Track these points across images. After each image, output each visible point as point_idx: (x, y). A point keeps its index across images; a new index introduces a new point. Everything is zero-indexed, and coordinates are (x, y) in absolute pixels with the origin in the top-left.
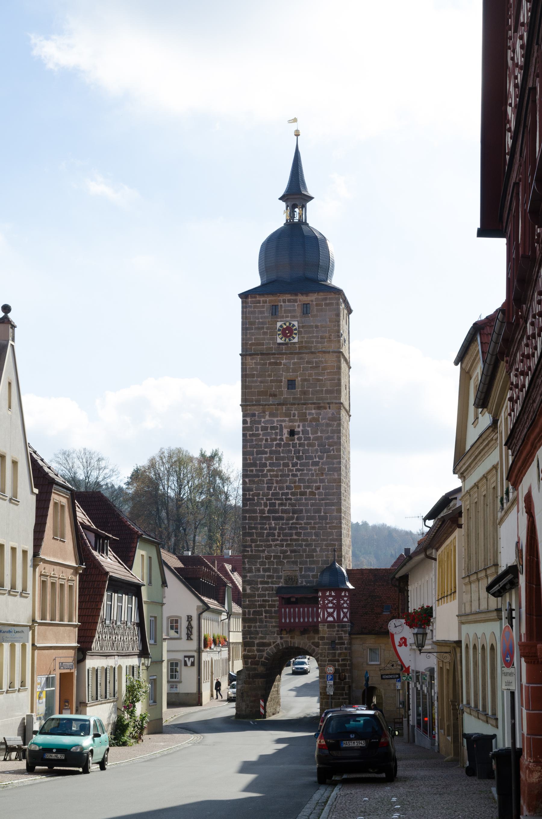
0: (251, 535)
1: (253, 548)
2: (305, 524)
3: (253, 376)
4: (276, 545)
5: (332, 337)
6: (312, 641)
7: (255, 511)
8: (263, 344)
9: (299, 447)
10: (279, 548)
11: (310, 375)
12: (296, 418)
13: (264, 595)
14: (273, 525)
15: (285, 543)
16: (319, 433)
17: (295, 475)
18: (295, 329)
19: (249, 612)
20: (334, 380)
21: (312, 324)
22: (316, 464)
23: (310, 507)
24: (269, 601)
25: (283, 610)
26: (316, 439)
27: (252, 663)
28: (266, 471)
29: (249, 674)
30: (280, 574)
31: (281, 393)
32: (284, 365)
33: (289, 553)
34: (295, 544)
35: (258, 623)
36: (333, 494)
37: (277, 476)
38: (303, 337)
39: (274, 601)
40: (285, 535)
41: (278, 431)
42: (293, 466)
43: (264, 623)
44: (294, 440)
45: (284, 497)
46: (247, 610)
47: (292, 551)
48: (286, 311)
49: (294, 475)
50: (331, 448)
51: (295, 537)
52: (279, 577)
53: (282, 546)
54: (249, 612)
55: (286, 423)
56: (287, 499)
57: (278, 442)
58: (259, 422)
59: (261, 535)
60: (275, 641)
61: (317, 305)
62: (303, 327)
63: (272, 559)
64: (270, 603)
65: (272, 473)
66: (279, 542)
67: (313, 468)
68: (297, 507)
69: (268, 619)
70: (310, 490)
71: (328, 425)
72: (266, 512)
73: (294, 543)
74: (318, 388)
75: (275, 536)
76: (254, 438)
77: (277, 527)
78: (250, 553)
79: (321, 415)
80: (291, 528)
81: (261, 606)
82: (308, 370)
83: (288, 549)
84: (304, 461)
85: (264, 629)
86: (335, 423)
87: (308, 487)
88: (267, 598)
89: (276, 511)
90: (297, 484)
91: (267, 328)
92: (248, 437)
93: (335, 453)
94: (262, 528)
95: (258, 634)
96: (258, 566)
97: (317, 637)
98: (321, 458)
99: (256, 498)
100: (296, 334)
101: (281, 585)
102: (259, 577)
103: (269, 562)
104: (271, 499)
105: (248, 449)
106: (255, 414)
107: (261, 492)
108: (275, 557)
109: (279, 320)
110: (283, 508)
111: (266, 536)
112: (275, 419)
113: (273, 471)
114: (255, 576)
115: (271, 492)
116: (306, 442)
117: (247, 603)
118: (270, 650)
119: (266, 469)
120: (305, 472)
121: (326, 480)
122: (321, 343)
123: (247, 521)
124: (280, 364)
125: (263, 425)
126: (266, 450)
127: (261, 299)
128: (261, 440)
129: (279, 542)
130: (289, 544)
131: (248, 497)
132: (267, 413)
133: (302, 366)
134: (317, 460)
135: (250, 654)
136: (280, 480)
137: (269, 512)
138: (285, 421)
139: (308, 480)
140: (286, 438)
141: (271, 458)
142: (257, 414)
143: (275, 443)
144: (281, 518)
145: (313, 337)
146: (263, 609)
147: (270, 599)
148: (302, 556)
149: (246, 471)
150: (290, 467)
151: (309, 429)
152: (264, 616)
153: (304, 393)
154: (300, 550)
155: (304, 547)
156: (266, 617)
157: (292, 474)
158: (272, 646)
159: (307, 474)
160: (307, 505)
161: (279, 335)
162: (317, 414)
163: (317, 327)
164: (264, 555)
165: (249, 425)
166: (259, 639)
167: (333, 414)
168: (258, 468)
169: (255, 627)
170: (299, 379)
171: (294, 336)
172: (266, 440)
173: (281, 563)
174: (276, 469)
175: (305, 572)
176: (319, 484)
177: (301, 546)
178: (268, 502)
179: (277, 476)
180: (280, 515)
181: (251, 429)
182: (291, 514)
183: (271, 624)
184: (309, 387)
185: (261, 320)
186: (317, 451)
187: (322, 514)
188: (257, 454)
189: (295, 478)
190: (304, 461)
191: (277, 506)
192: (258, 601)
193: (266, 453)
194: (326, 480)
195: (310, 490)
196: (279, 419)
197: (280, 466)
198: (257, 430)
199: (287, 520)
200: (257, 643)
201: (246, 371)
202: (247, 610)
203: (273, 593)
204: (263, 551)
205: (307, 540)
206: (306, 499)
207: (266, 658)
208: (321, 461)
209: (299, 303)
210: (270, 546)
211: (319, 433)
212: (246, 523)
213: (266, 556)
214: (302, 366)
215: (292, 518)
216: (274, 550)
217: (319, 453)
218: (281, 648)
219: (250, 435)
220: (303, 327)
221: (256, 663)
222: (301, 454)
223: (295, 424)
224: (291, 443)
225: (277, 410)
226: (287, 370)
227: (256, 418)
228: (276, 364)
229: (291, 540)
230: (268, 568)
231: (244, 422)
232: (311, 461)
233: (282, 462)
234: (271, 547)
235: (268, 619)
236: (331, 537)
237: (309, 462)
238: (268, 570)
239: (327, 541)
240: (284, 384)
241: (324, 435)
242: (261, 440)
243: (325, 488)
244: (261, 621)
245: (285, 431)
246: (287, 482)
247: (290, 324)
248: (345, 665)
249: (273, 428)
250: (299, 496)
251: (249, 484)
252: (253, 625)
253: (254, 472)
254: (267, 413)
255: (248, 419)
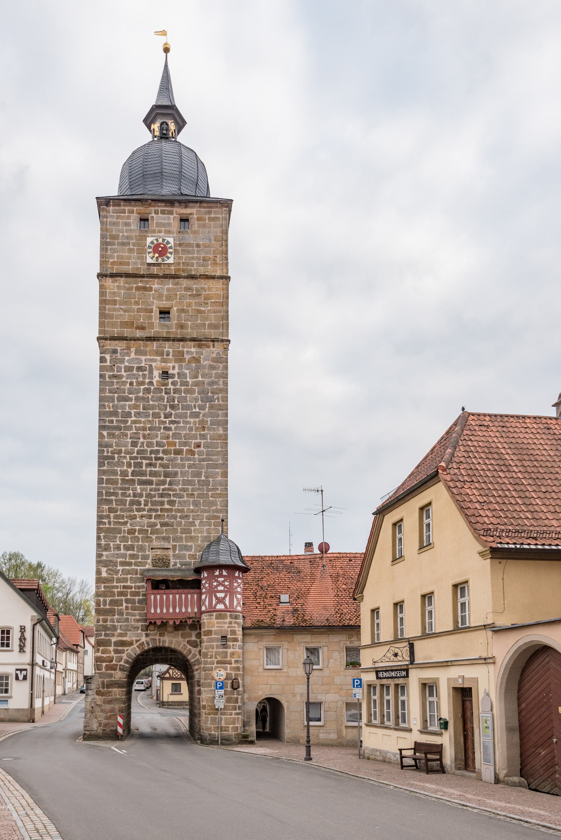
0: (110, 502)
1: (112, 520)
2: (181, 490)
3: (115, 302)
4: (142, 516)
5: (218, 259)
6: (187, 640)
7: (115, 473)
8: (128, 264)
9: (174, 393)
10: (145, 520)
11: (189, 305)
12: (171, 357)
13: (126, 580)
14: (139, 491)
15: (154, 514)
16: (200, 377)
17: (169, 429)
18: (171, 248)
19: (105, 601)
20: (219, 312)
21: (192, 242)
22: (196, 415)
23: (187, 469)
24: (131, 588)
25: (152, 597)
26: (197, 384)
27: (107, 668)
28: (130, 422)
29: (103, 683)
30: (147, 553)
31: (152, 325)
32: (156, 291)
33: (159, 527)
34: (168, 515)
35: (117, 616)
36: (218, 453)
37: (144, 429)
38: (180, 258)
39: (139, 587)
40: (154, 503)
41: (146, 373)
42: (165, 417)
43: (125, 616)
44: (167, 385)
45: (153, 456)
46: (102, 599)
47: (162, 525)
48: (158, 225)
49: (167, 429)
50: (215, 397)
51: (167, 506)
52: (145, 557)
53: (150, 517)
54: (105, 601)
55: (158, 364)
56: (156, 459)
57: (146, 386)
58: (122, 361)
59: (123, 502)
60: (138, 639)
61: (199, 219)
62: (180, 245)
63: (136, 534)
64: (133, 590)
65: (137, 425)
66: (145, 513)
67: (192, 420)
68: (171, 469)
69: (130, 611)
70: (187, 448)
71: (212, 367)
72: (130, 474)
73: (166, 514)
74: (199, 322)
75: (141, 505)
76: (115, 381)
77: (144, 493)
78: (107, 526)
79: (202, 354)
80: (162, 496)
81: (121, 594)
82: (186, 299)
83: (158, 521)
84: (180, 411)
85: (125, 624)
86: (221, 366)
87: (185, 444)
88: (129, 584)
89: (143, 474)
90: (171, 440)
91: (134, 245)
92: (107, 379)
93: (221, 402)
94: (123, 495)
95: (116, 630)
96: (118, 542)
97: (194, 633)
98: (202, 408)
99: (116, 456)
100: (171, 253)
101: (147, 567)
102: (118, 556)
103: (131, 538)
104: (136, 458)
105: (107, 394)
106: (117, 350)
107: (123, 449)
108: (140, 531)
109: (150, 235)
110: (152, 469)
111: (129, 504)
112: (143, 358)
113: (140, 422)
114: (113, 555)
115: (136, 449)
116: (183, 388)
117: (103, 589)
118: (133, 651)
119: (129, 420)
120: (182, 425)
121: (208, 437)
122: (203, 266)
123: (104, 485)
124: (150, 289)
125: (127, 364)
126: (131, 396)
127: (127, 208)
128: (124, 383)
129: (145, 513)
130: (160, 515)
131: (105, 454)
132: (133, 350)
133: (178, 293)
134: (197, 410)
135: (105, 655)
136: (149, 435)
137: (133, 474)
138: (155, 361)
139: (186, 435)
140: (157, 381)
141: (136, 407)
142: (119, 351)
143: (142, 387)
144: (150, 483)
145: (193, 258)
146: (124, 598)
147: (133, 585)
148: (175, 531)
149: (104, 421)
150: (162, 419)
151: (187, 372)
152: (124, 607)
153: (182, 327)
154: (173, 523)
155: (178, 519)
156: (127, 608)
157: (164, 428)
158: (135, 646)
159: (184, 428)
160: (183, 466)
161: (149, 253)
162: (197, 352)
163: (198, 246)
164: (126, 529)
165: (108, 364)
166: (118, 636)
167: (218, 353)
168: (120, 418)
169: (112, 620)
170: (175, 309)
171: (169, 255)
172: (131, 384)
173: (148, 539)
174: (143, 420)
175: (179, 550)
176: (199, 441)
177: (175, 517)
178: (132, 461)
179: (144, 429)
180: (148, 478)
181: (111, 368)
182: (162, 478)
183: (133, 618)
184: (188, 320)
185: (125, 234)
186: (196, 400)
187: (203, 478)
188: (119, 401)
189: (169, 432)
190: (180, 411)
191: (144, 466)
192: (117, 587)
193: (131, 400)
194: (208, 437)
195: (187, 448)
196: (148, 357)
197: (148, 416)
198: (119, 370)
199: (156, 485)
200: (115, 642)
201: (106, 296)
202: (102, 599)
203: (137, 578)
204: (126, 523)
205: (182, 511)
206: (182, 459)
207: (127, 662)
208: (202, 412)
209: (175, 215)
210: (135, 517)
211: (200, 377)
212: (103, 488)
213: (128, 530)
214: (178, 293)
215: (164, 483)
216: (139, 522)
217: (200, 402)
218: (146, 648)
219: (110, 377)
220: (180, 245)
221: (114, 668)
222: (176, 402)
223: (169, 364)
224: (163, 388)
225: (146, 346)
226: (160, 297)
227: (119, 356)
228: (145, 289)
229: (162, 510)
230: (132, 545)
231: (102, 360)
232: (189, 412)
233: (151, 412)
234: (135, 518)
235: (130, 611)
236: (214, 508)
237: (186, 413)
238: (131, 548)
239: (209, 512)
240: (156, 314)
241: (206, 380)
242: (124, 383)
243: (207, 446)
244: (121, 613)
245: (156, 373)
246: (157, 436)
247: (164, 240)
248: (238, 669)
249: (140, 369)
250: (172, 455)
251: (108, 438)
252: (109, 618)
253: (115, 424)
254: (133, 350)
255: (108, 357)
